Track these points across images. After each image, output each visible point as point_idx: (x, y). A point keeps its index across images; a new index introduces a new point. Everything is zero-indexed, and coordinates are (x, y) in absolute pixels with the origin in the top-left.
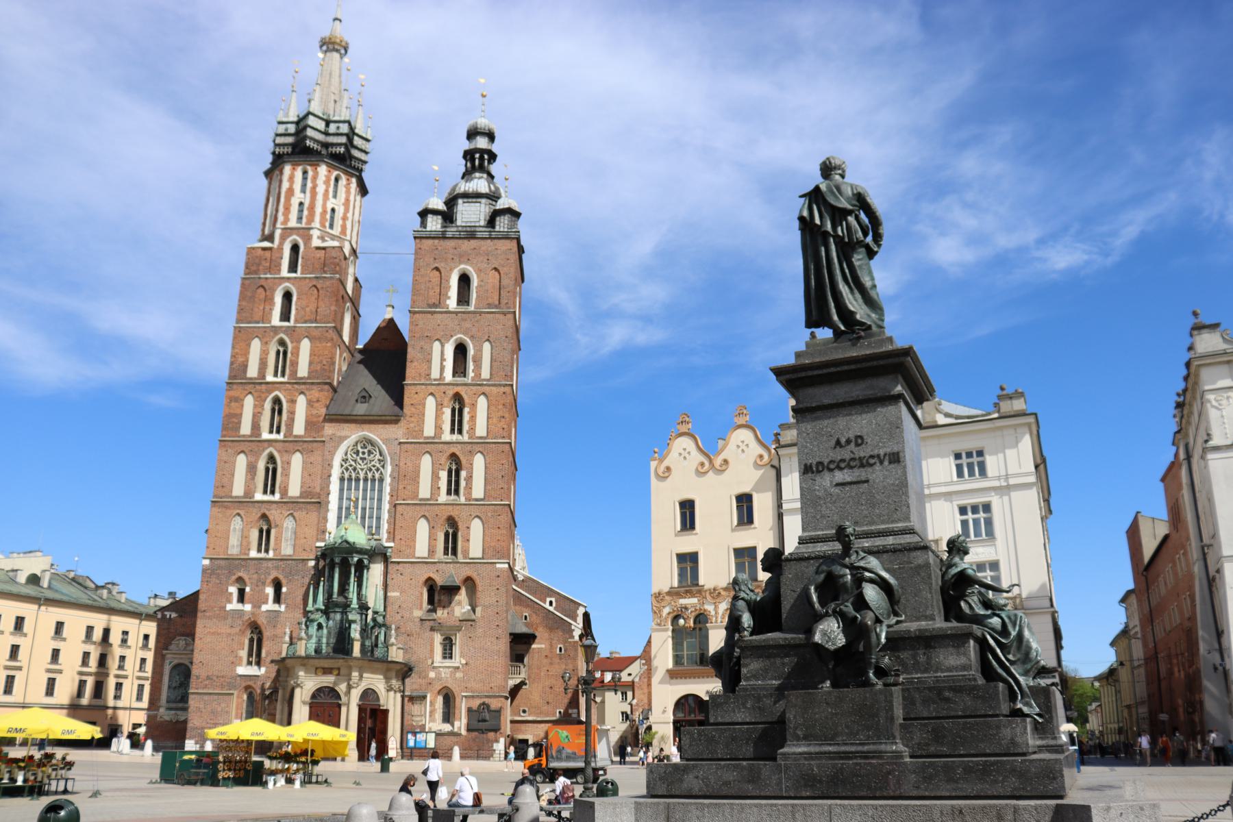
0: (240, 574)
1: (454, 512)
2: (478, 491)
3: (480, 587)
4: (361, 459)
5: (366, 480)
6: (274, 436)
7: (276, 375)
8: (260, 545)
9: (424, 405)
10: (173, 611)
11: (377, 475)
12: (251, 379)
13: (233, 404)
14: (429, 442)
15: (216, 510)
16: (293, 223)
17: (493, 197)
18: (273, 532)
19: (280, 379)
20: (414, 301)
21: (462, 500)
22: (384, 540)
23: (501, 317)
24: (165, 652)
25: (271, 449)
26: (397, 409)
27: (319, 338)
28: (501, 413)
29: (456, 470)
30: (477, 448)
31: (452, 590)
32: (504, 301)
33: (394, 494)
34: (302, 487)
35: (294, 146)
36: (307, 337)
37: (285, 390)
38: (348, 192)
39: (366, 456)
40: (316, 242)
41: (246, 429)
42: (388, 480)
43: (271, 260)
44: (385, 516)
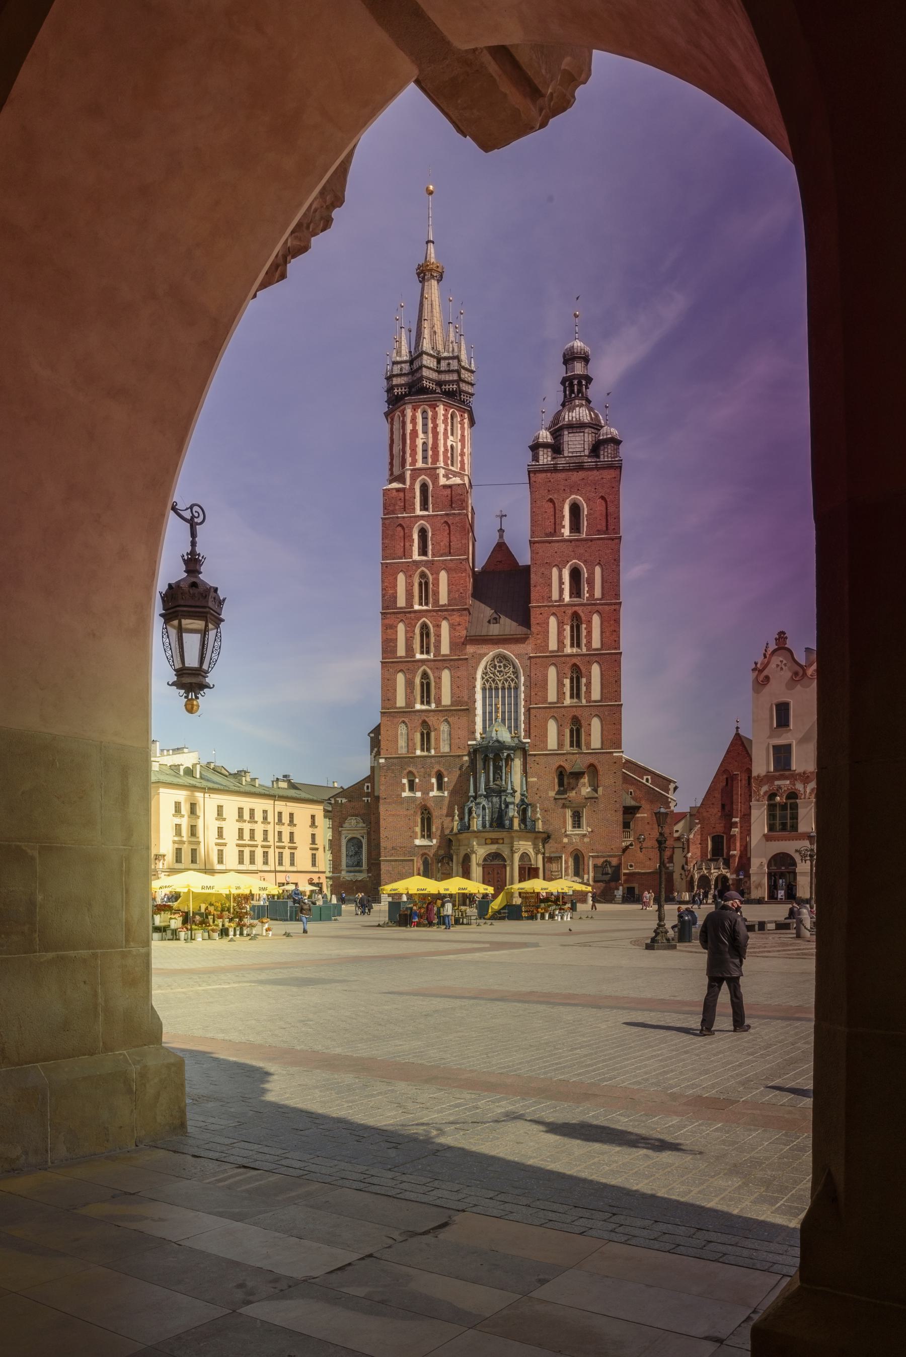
1: (577, 712)
2: (596, 694)
4: (498, 671)
5: (503, 688)
6: (425, 656)
7: (421, 604)
8: (422, 744)
11: (513, 685)
12: (401, 608)
15: (385, 719)
16: (420, 464)
17: (595, 426)
18: (433, 734)
19: (425, 608)
20: (533, 532)
22: (522, 737)
23: (610, 542)
24: (340, 829)
25: (424, 667)
26: (525, 630)
27: (455, 569)
29: (577, 674)
30: (595, 658)
31: (578, 775)
33: (528, 699)
34: (452, 697)
35: (410, 386)
36: (444, 569)
37: (431, 616)
38: (463, 428)
39: (502, 669)
40: (443, 481)
41: (401, 651)
42: (523, 688)
43: (405, 499)
44: (523, 718)
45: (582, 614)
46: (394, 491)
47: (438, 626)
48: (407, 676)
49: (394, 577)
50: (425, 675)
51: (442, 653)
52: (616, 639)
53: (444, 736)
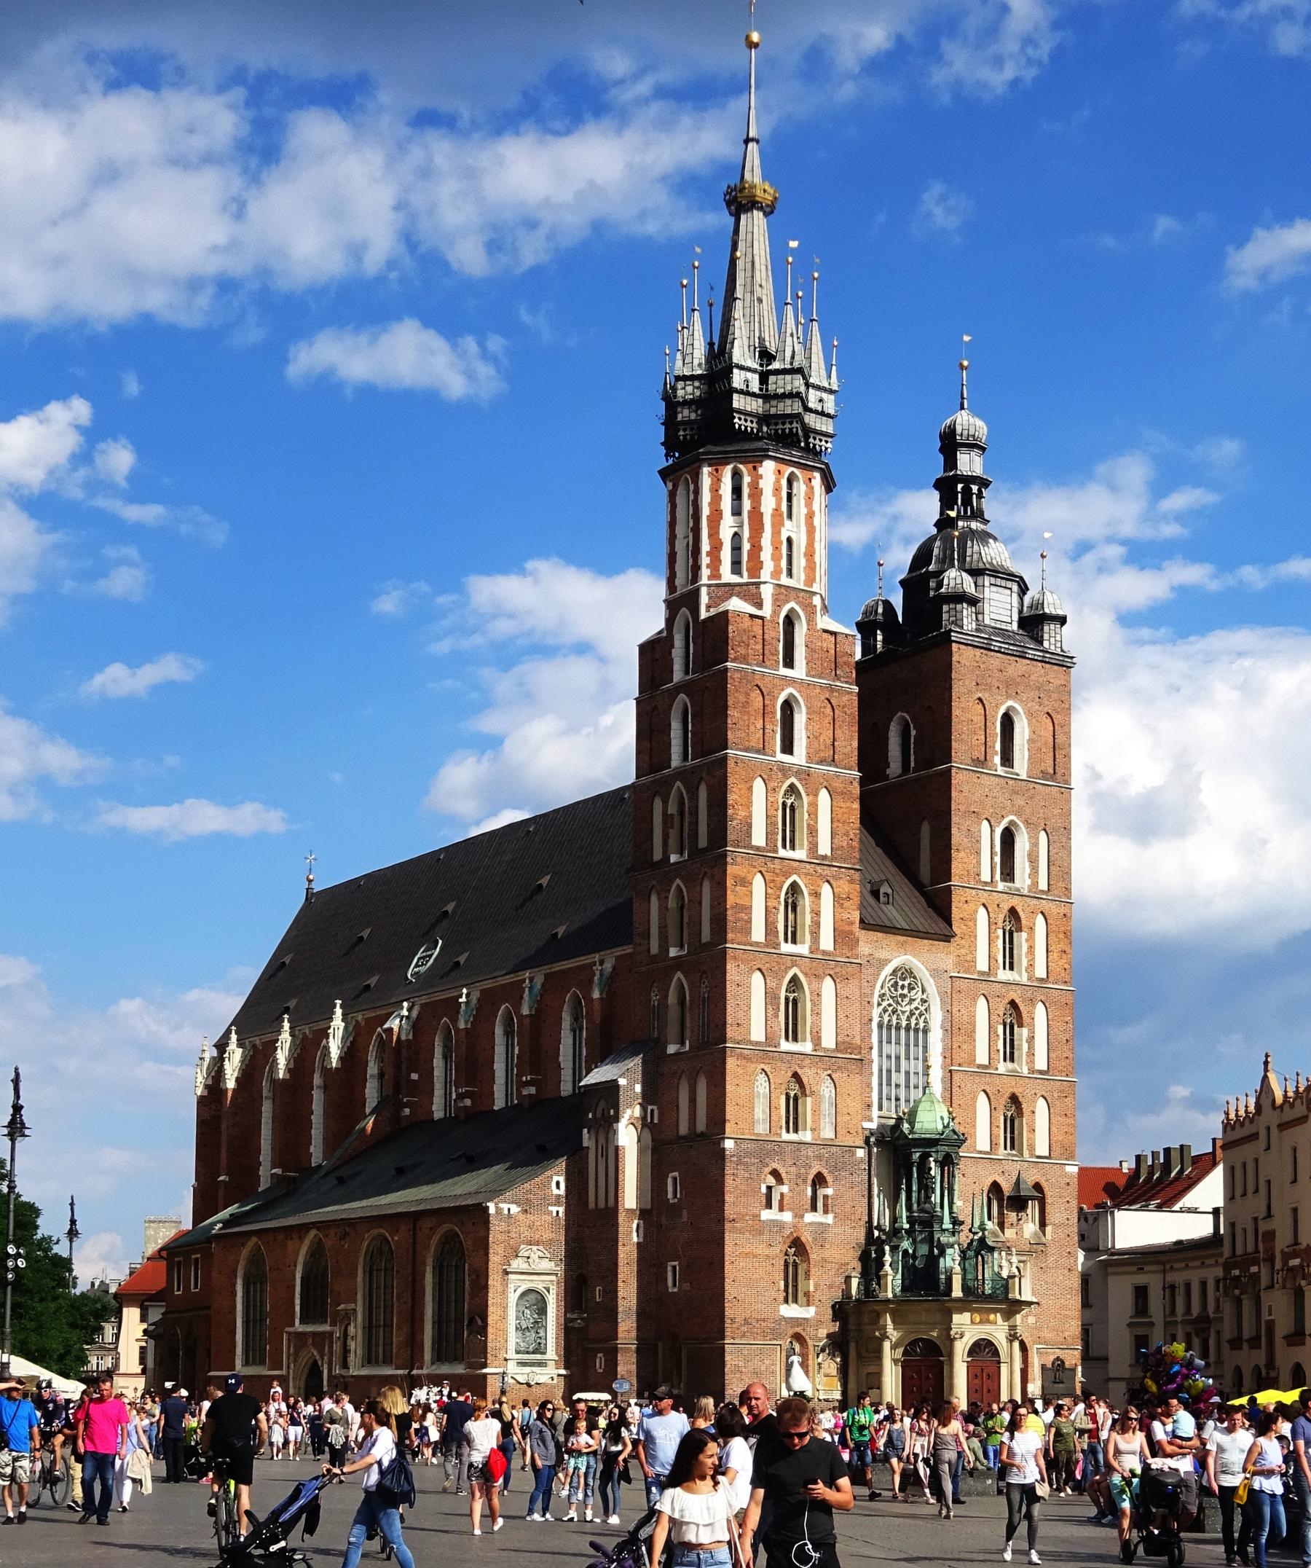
0: (775, 1165)
3: (1049, 1200)
7: (784, 846)
9: (975, 920)
10: (512, 1203)
11: (922, 1025)
12: (758, 848)
13: (738, 888)
14: (986, 977)
21: (1025, 1071)
25: (795, 970)
26: (943, 924)
28: (1062, 946)
32: (1060, 771)
34: (837, 1035)
39: (906, 991)
45: (1021, 914)
46: (747, 622)
47: (816, 895)
48: (768, 981)
49: (748, 785)
50: (795, 983)
51: (822, 947)
52: (1067, 966)
53: (827, 1108)
